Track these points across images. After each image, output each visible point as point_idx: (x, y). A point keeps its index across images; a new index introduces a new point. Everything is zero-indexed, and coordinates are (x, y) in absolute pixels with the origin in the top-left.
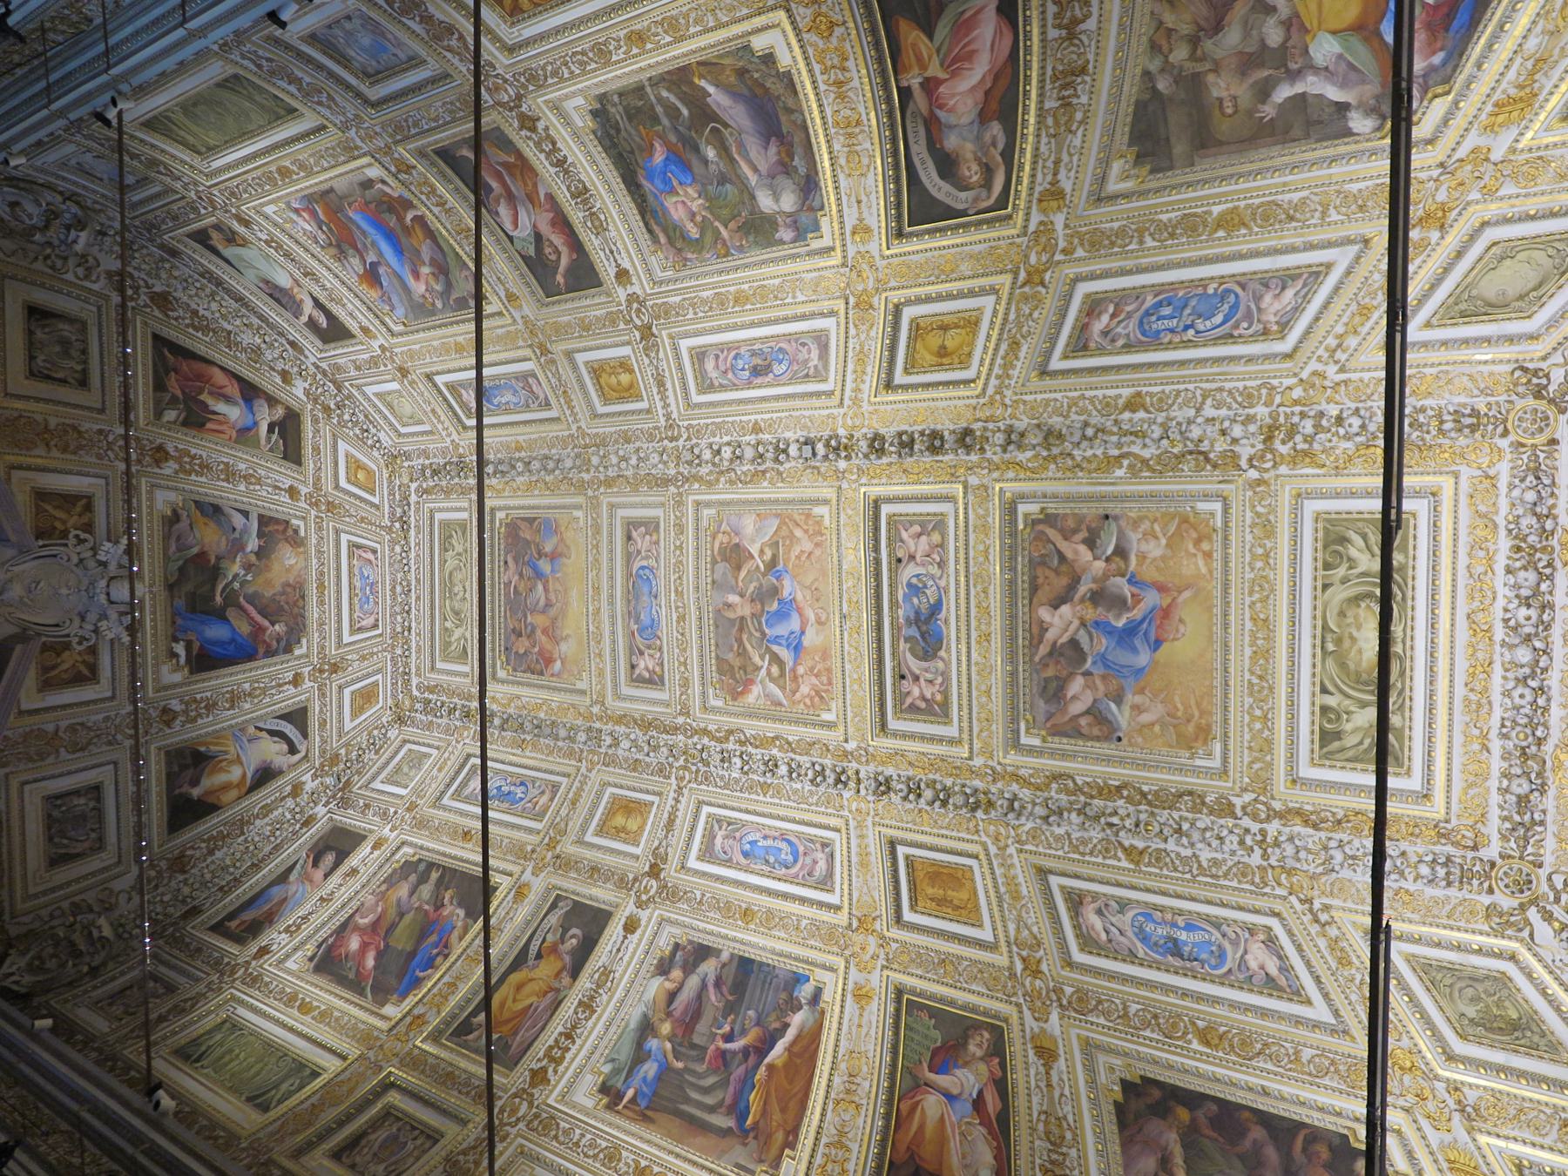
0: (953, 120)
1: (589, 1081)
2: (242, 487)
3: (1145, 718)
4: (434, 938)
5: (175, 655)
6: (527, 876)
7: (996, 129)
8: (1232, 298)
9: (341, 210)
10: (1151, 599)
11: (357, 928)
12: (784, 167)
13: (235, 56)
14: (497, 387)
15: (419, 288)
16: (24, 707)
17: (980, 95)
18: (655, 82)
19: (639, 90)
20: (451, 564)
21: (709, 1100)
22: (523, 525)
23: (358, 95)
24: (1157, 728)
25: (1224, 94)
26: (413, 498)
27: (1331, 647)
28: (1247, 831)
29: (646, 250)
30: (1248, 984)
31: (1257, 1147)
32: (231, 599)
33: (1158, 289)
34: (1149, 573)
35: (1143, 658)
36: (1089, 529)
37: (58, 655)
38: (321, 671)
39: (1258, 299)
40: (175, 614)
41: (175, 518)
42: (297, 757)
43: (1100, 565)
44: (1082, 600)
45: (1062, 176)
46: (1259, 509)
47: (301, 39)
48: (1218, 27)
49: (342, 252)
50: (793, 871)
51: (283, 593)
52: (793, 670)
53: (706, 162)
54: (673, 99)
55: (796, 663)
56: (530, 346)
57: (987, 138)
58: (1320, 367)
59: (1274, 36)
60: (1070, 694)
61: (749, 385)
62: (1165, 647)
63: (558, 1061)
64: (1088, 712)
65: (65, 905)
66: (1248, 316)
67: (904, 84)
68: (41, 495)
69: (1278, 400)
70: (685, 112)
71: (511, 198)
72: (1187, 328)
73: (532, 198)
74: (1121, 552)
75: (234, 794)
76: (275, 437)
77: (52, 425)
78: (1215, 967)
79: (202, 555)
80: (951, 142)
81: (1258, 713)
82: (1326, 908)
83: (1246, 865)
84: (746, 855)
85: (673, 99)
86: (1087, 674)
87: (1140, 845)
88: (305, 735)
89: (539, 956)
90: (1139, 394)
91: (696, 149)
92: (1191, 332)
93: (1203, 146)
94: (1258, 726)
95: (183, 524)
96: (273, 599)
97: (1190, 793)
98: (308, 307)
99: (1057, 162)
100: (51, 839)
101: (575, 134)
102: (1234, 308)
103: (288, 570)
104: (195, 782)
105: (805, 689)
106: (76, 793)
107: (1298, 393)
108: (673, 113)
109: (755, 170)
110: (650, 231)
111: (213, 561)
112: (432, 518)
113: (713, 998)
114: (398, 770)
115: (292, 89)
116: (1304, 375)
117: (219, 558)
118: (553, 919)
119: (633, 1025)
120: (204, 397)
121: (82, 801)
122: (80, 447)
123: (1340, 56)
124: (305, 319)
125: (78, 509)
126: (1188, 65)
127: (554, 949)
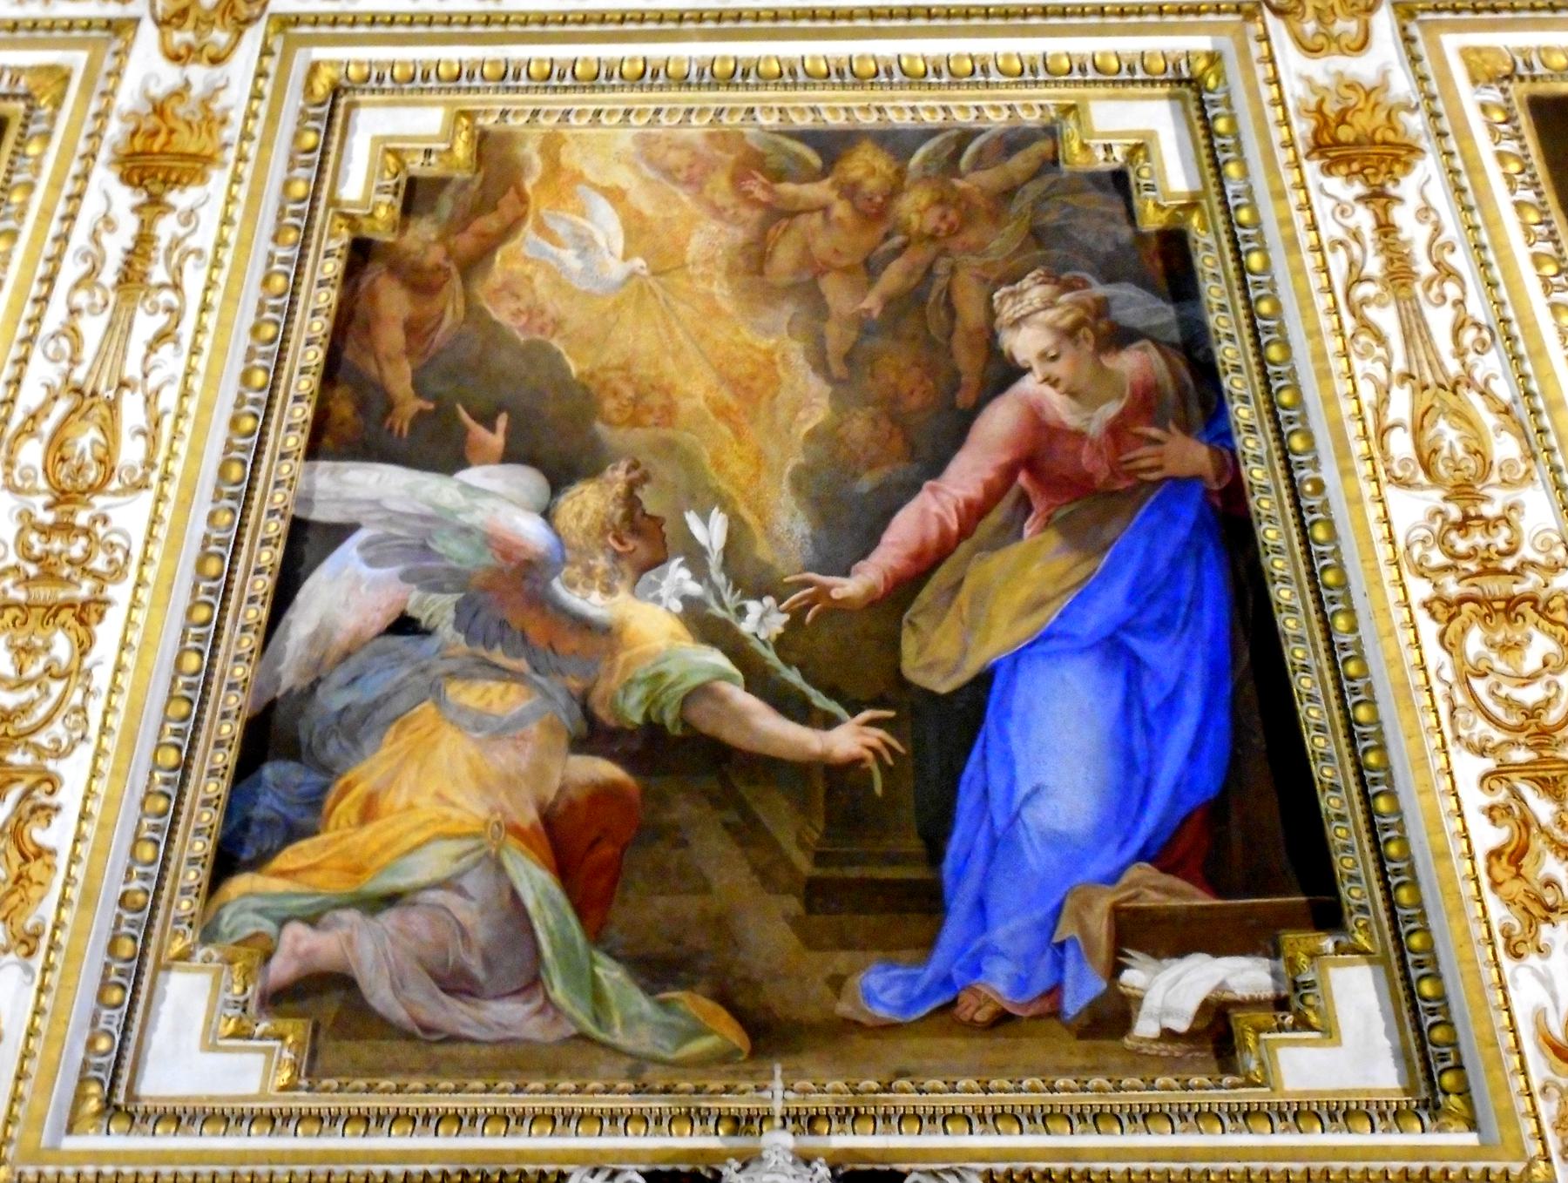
51: (808, 292)
111: (605, 770)
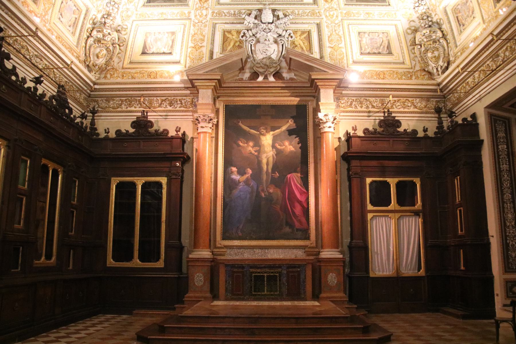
37: (296, 46)
77: (193, 45)
100: (379, 53)
121: (364, 39)
122: (202, 34)
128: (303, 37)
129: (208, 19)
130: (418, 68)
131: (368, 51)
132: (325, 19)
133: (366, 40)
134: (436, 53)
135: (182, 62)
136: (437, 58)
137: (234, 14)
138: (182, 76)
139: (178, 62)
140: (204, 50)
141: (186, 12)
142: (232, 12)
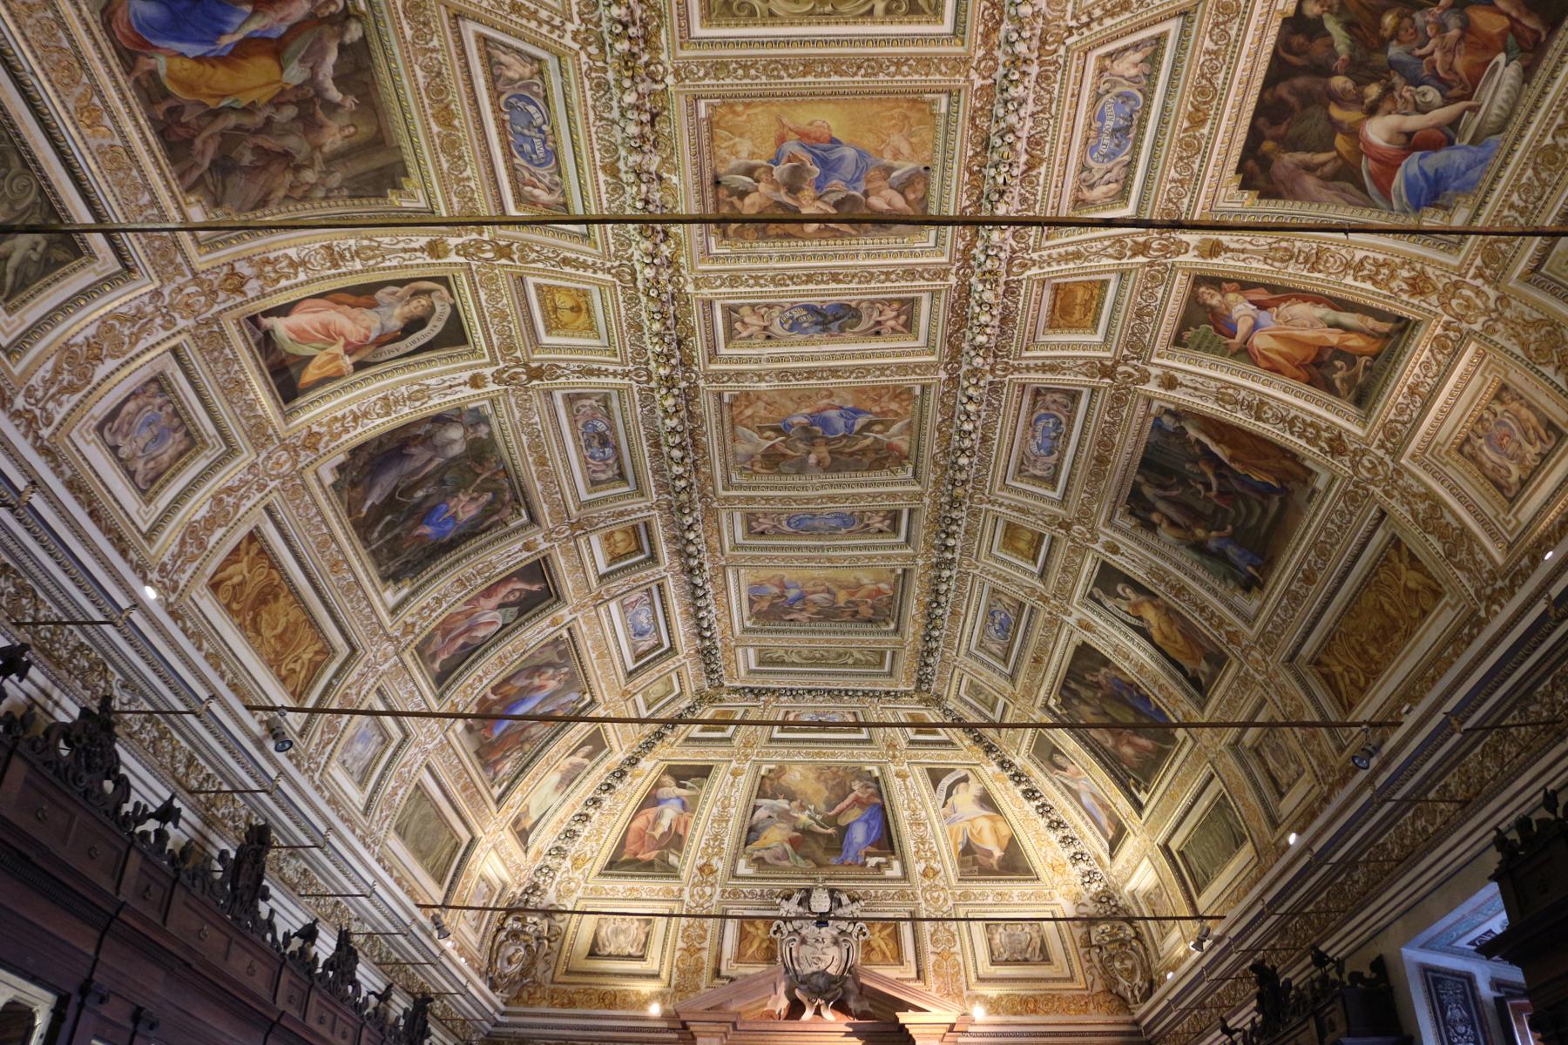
0: (378, 325)
1: (1239, 599)
2: (733, 811)
3: (905, 149)
4: (1125, 694)
5: (878, 866)
6: (1071, 620)
7: (380, 295)
8: (513, 100)
9: (491, 744)
10: (792, 147)
11: (1115, 747)
12: (426, 440)
13: (381, 834)
14: (634, 626)
15: (552, 685)
16: (914, 975)
17: (355, 312)
18: (366, 541)
19: (374, 554)
20: (795, 659)
21: (1258, 511)
22: (756, 607)
23: (400, 747)
24: (913, 140)
25: (339, 136)
26: (738, 684)
27: (828, 8)
28: (1006, 76)
29: (506, 530)
30: (1151, 77)
31: (1295, 91)
32: (831, 821)
33: (508, 156)
34: (769, 149)
35: (849, 153)
36: (730, 196)
38: (894, 757)
39: (511, 81)
40: (842, 863)
41: (760, 862)
42: (970, 775)
43: (762, 187)
44: (797, 199)
45: (416, 245)
46: (701, 73)
47: (363, 789)
48: (286, 155)
49: (527, 740)
50: (1064, 420)
51: (826, 781)
52: (876, 414)
53: (426, 497)
54: (379, 528)
55: (870, 412)
56: (595, 607)
57: (388, 299)
58: (568, 36)
59: (290, 112)
60: (886, 207)
61: (616, 448)
62: (834, 135)
63: (1221, 623)
64: (902, 193)
65: (1082, 951)
66: (527, 87)
67: (351, 368)
68: (740, 957)
69: (600, 64)
70: (389, 518)
71: (470, 629)
72: (541, 131)
73: (469, 615)
74: (750, 171)
75: (1002, 827)
76: (689, 784)
78: (1136, 99)
79: (792, 841)
80: (395, 324)
81: (893, 69)
82: (1075, 17)
83: (1039, 76)
84: (1050, 453)
85: (379, 528)
86: (866, 194)
87: (1024, 158)
88: (953, 770)
89: (1140, 618)
90: (603, 168)
91: (419, 505)
92: (545, 128)
93: (383, 142)
94: (905, 69)
95: (765, 854)
96: (831, 790)
97: (973, 119)
98: (577, 759)
99: (405, 250)
100: (1026, 960)
101: (414, 593)
102: (521, 98)
103: (806, 778)
104: (990, 854)
105: (894, 406)
106: (990, 940)
107: (593, 50)
108: (390, 526)
109: (431, 460)
110: (489, 528)
112: (755, 672)
113: (1175, 493)
114: (984, 702)
115: (401, 792)
116: (576, 46)
117: (796, 830)
118: (1109, 603)
119: (1197, 557)
120: (657, 834)
121: (997, 937)
122: (701, 927)
123: (302, 61)
124: (586, 761)
125: (752, 930)
126: (317, 168)
127: (1135, 606)
128: (885, 933)
129: (714, 901)
130: (1098, 987)
131: (1005, 956)
132: (923, 905)
133: (1000, 936)
134: (1128, 964)
135: (664, 975)
136: (1133, 971)
137: (762, 895)
138: (663, 1003)
139: (655, 976)
140: (705, 955)
141: (675, 888)
142: (758, 891)
